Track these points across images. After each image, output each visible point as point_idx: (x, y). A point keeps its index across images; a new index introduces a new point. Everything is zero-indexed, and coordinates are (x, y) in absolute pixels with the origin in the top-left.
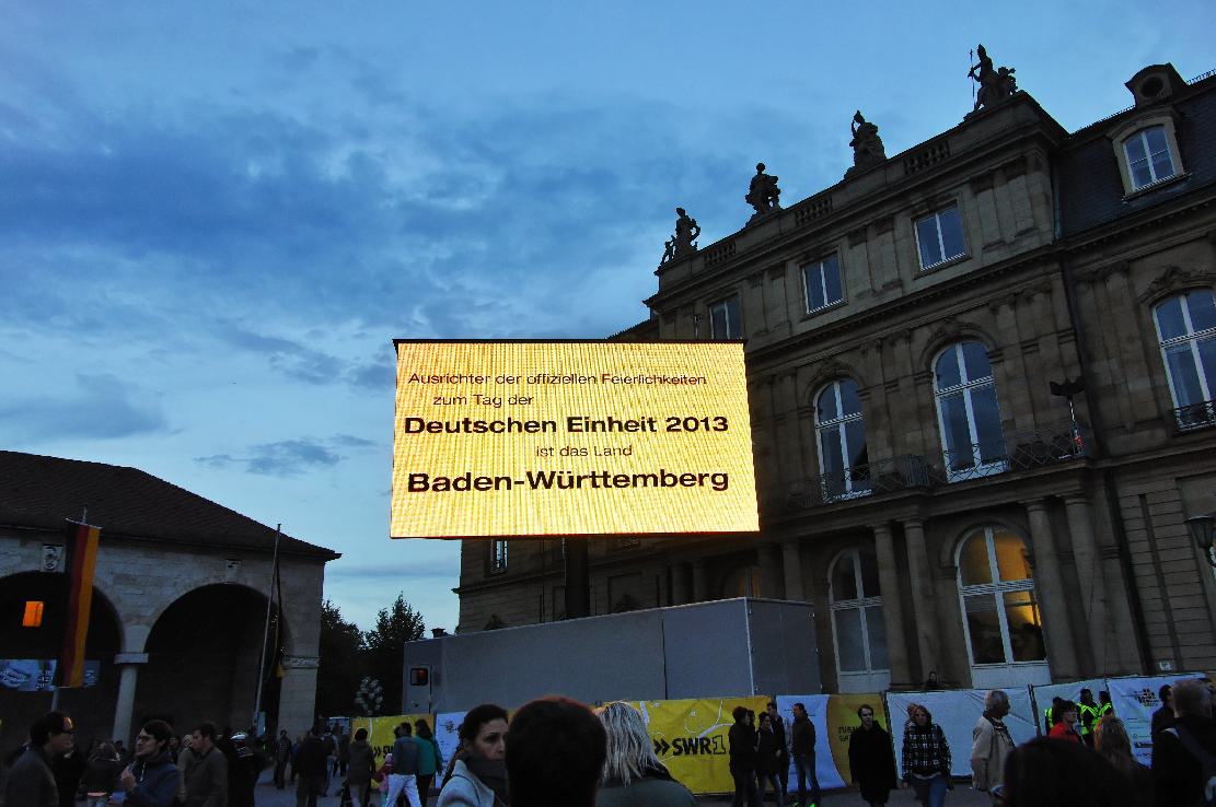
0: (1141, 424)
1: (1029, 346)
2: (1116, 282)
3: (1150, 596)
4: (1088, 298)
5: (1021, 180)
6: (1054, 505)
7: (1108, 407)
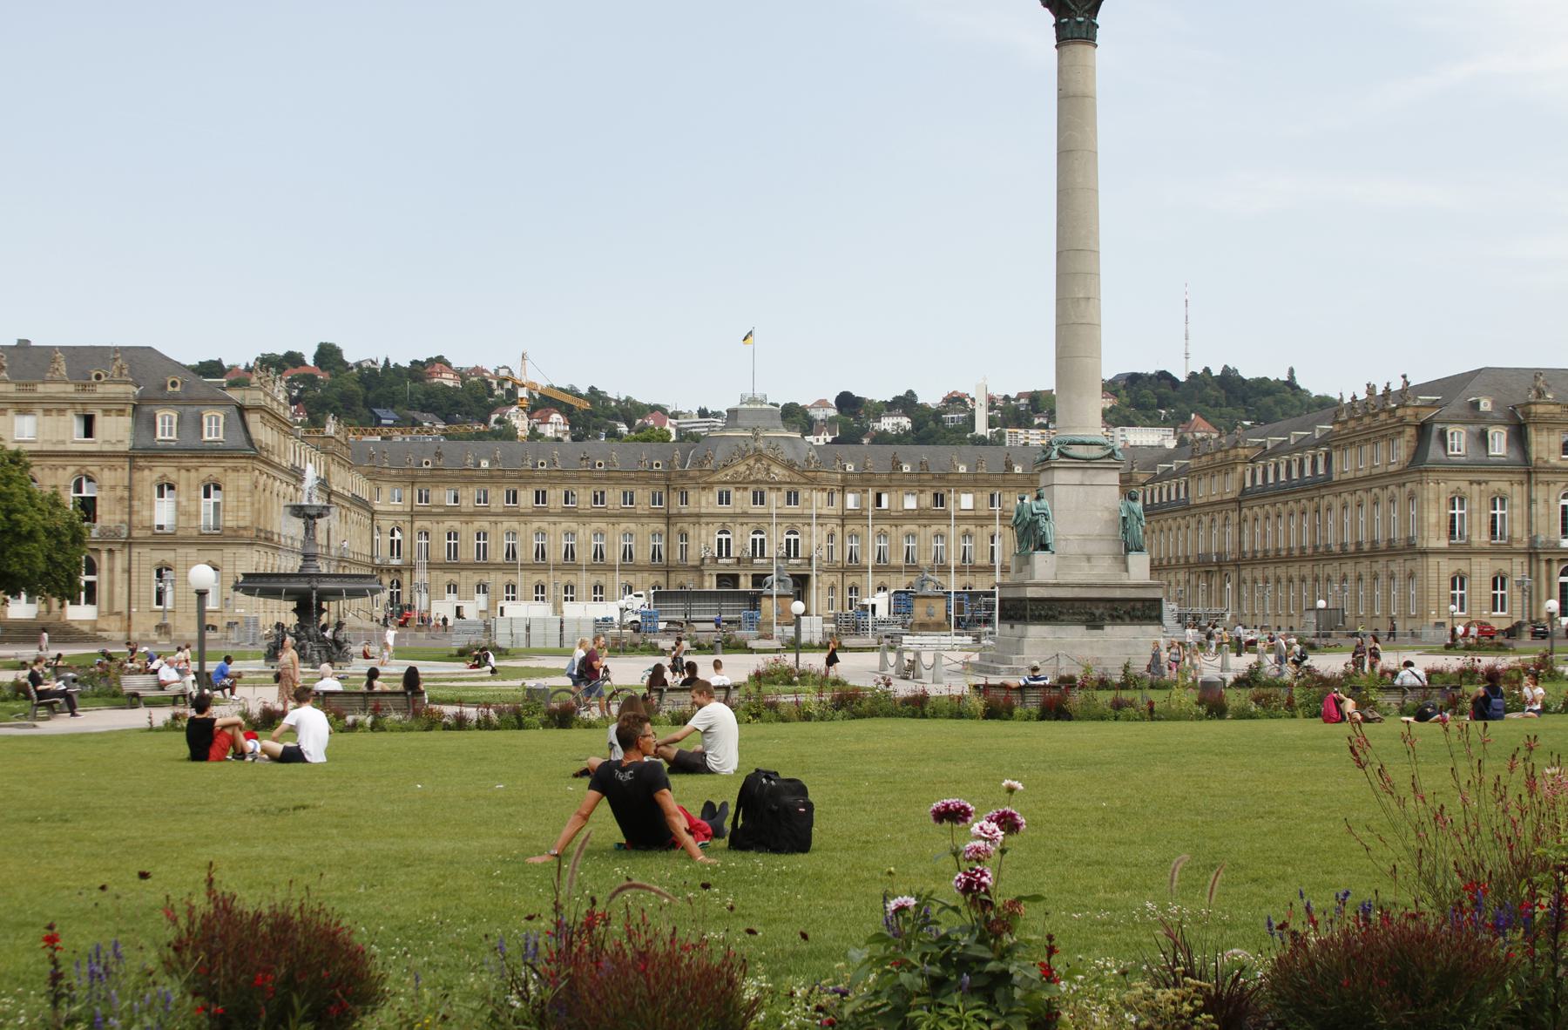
0: (144, 528)
1: (113, 488)
2: (147, 472)
3: (134, 587)
4: (137, 475)
5: (121, 419)
6: (110, 551)
7: (135, 518)
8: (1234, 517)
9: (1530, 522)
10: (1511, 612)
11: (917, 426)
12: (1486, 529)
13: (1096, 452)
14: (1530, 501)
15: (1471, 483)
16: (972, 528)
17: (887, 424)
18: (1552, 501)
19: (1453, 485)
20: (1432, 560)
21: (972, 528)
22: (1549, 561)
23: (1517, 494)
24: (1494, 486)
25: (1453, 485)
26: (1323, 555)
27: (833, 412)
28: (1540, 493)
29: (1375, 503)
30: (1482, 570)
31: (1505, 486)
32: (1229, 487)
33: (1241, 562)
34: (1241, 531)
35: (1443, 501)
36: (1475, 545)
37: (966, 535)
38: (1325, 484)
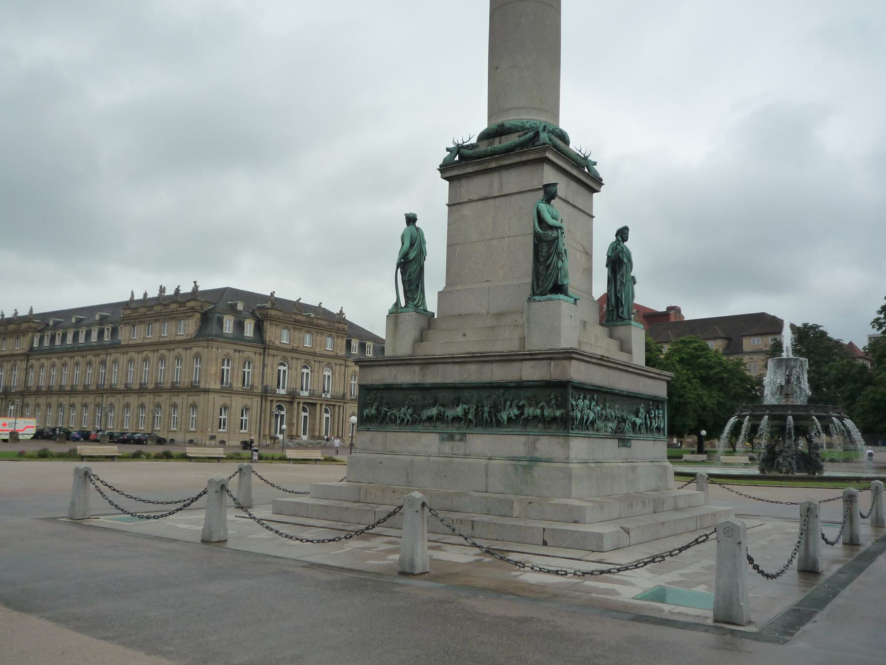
8: (24, 365)
9: (263, 378)
10: (250, 430)
12: (240, 380)
14: (264, 365)
15: (235, 351)
18: (275, 366)
19: (225, 351)
20: (211, 396)
23: (258, 360)
24: (246, 354)
25: (225, 351)
26: (101, 391)
28: (269, 360)
29: (77, 364)
30: (237, 403)
31: (252, 355)
33: (25, 393)
34: (27, 374)
35: (220, 360)
36: (235, 389)
38: (116, 346)
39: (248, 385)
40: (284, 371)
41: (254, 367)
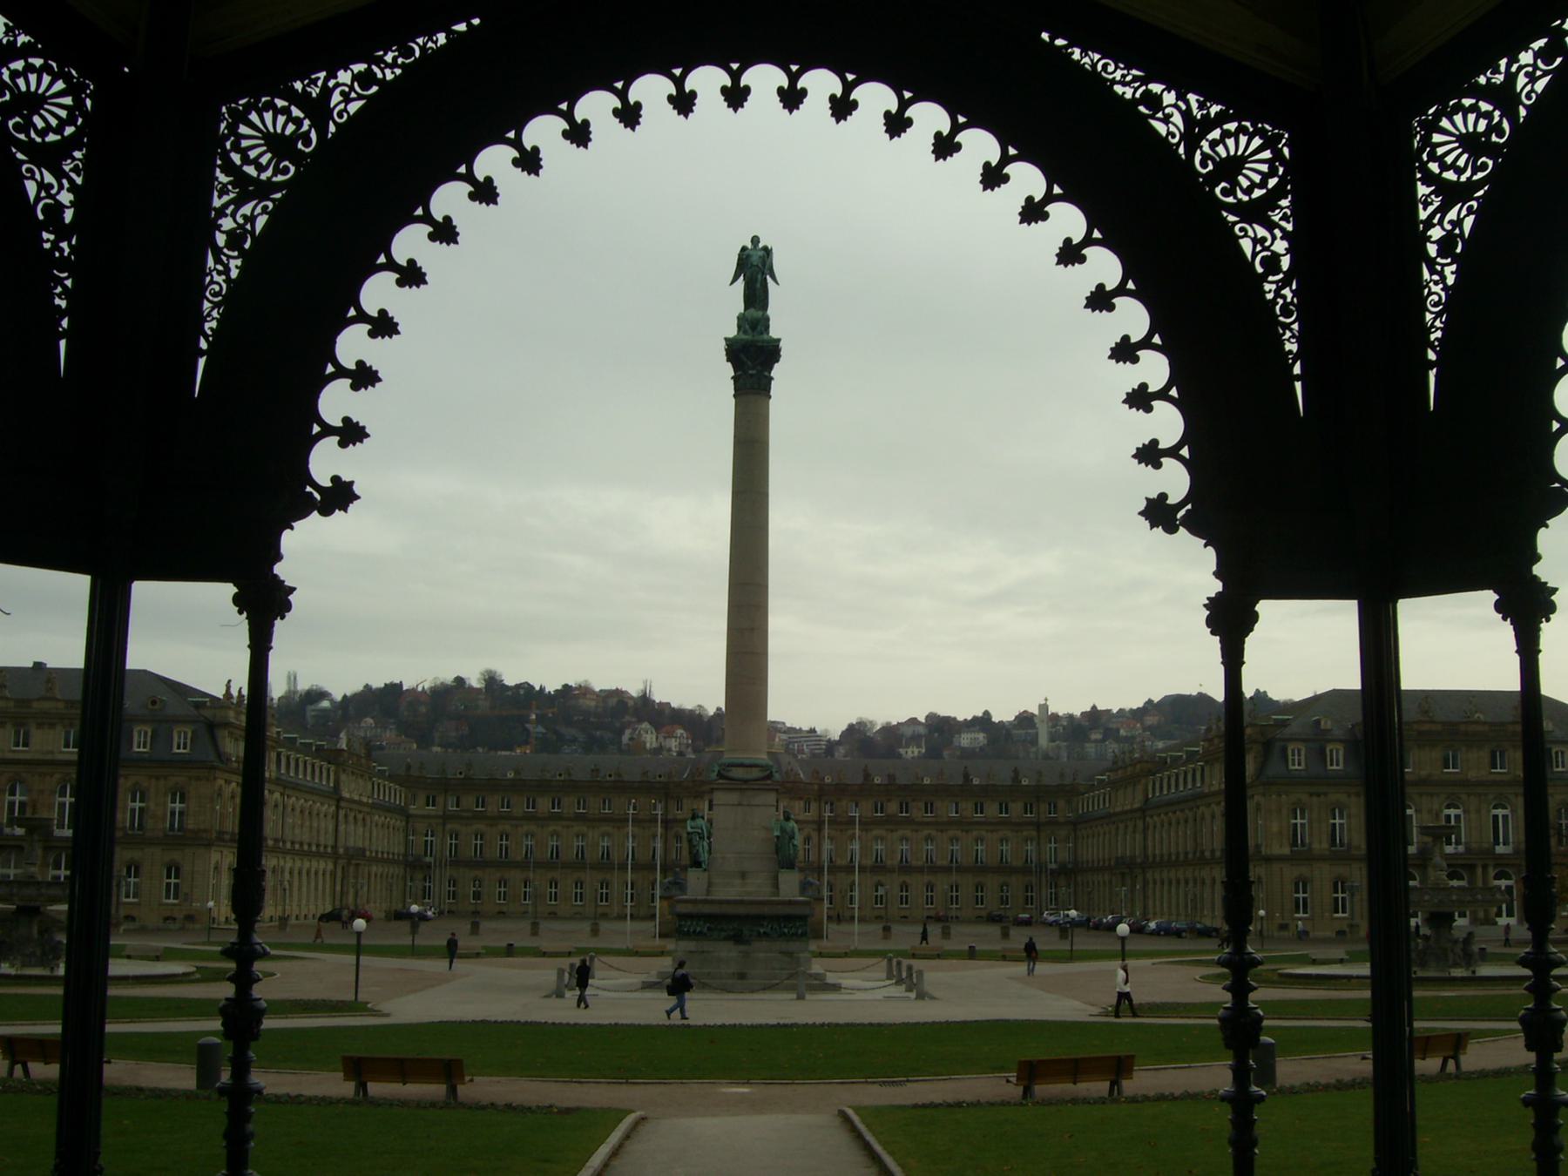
8: (1140, 824)
10: (1352, 914)
11: (992, 741)
13: (756, 773)
15: (1311, 795)
16: (933, 833)
17: (965, 740)
21: (933, 833)
22: (1485, 867)
27: (922, 730)
30: (1323, 874)
32: (1128, 800)
34: (1145, 839)
37: (929, 838)
39: (1342, 845)
40: (1505, 817)
41: (1349, 816)
